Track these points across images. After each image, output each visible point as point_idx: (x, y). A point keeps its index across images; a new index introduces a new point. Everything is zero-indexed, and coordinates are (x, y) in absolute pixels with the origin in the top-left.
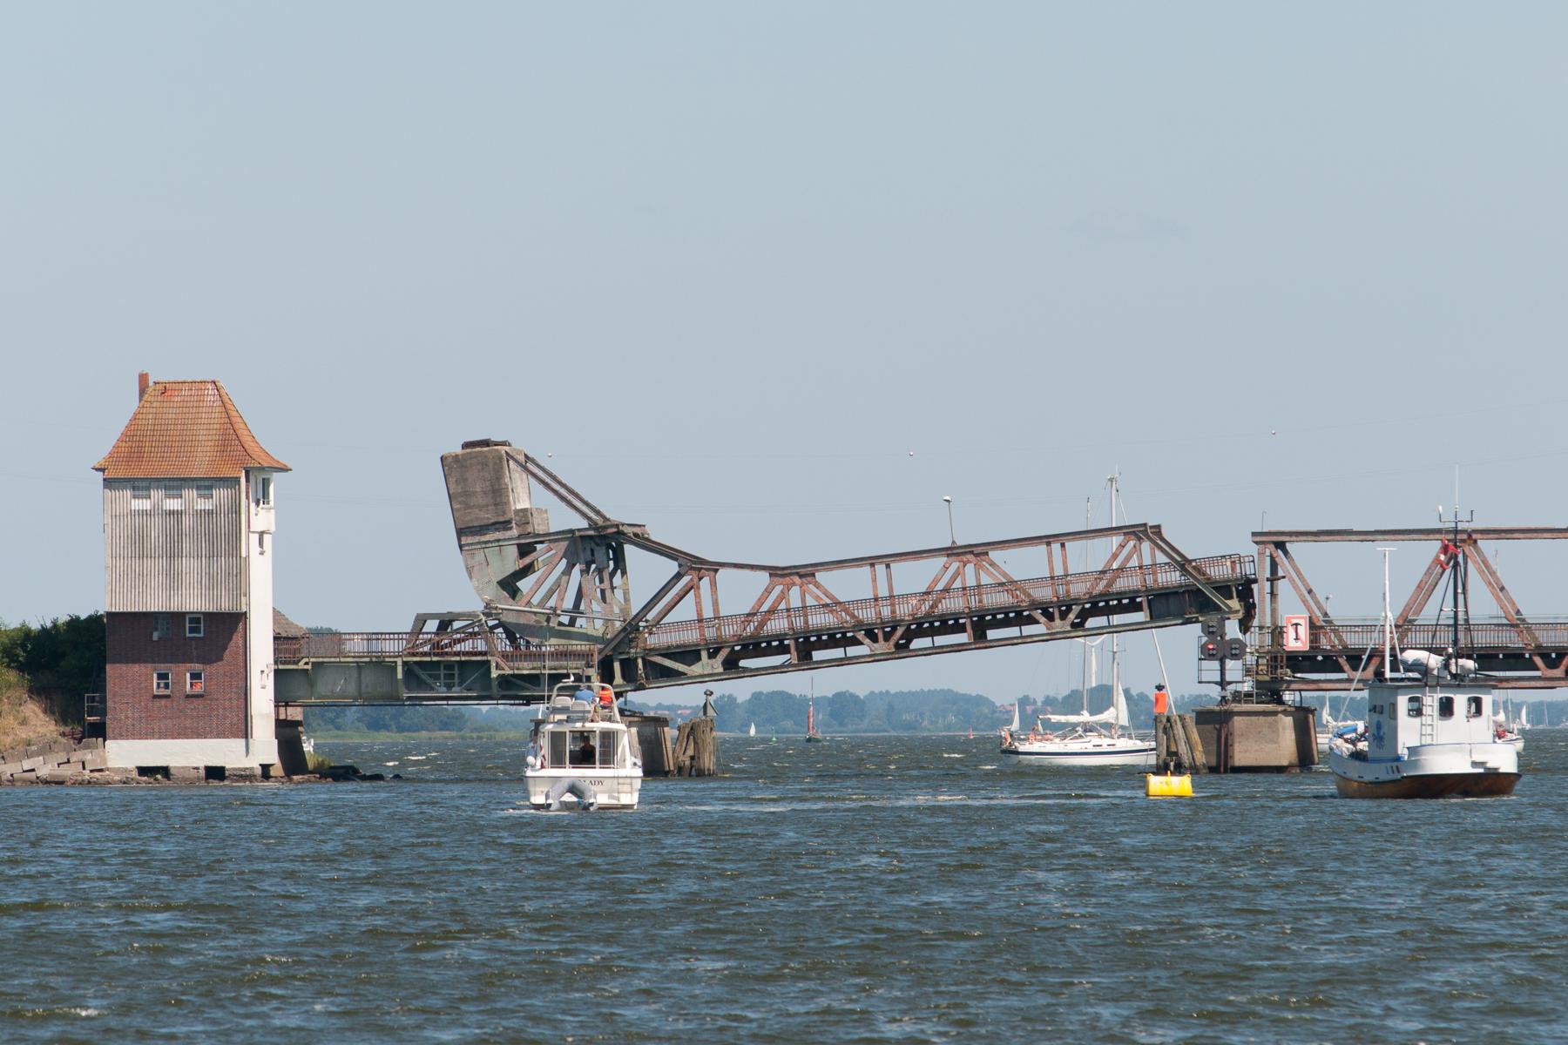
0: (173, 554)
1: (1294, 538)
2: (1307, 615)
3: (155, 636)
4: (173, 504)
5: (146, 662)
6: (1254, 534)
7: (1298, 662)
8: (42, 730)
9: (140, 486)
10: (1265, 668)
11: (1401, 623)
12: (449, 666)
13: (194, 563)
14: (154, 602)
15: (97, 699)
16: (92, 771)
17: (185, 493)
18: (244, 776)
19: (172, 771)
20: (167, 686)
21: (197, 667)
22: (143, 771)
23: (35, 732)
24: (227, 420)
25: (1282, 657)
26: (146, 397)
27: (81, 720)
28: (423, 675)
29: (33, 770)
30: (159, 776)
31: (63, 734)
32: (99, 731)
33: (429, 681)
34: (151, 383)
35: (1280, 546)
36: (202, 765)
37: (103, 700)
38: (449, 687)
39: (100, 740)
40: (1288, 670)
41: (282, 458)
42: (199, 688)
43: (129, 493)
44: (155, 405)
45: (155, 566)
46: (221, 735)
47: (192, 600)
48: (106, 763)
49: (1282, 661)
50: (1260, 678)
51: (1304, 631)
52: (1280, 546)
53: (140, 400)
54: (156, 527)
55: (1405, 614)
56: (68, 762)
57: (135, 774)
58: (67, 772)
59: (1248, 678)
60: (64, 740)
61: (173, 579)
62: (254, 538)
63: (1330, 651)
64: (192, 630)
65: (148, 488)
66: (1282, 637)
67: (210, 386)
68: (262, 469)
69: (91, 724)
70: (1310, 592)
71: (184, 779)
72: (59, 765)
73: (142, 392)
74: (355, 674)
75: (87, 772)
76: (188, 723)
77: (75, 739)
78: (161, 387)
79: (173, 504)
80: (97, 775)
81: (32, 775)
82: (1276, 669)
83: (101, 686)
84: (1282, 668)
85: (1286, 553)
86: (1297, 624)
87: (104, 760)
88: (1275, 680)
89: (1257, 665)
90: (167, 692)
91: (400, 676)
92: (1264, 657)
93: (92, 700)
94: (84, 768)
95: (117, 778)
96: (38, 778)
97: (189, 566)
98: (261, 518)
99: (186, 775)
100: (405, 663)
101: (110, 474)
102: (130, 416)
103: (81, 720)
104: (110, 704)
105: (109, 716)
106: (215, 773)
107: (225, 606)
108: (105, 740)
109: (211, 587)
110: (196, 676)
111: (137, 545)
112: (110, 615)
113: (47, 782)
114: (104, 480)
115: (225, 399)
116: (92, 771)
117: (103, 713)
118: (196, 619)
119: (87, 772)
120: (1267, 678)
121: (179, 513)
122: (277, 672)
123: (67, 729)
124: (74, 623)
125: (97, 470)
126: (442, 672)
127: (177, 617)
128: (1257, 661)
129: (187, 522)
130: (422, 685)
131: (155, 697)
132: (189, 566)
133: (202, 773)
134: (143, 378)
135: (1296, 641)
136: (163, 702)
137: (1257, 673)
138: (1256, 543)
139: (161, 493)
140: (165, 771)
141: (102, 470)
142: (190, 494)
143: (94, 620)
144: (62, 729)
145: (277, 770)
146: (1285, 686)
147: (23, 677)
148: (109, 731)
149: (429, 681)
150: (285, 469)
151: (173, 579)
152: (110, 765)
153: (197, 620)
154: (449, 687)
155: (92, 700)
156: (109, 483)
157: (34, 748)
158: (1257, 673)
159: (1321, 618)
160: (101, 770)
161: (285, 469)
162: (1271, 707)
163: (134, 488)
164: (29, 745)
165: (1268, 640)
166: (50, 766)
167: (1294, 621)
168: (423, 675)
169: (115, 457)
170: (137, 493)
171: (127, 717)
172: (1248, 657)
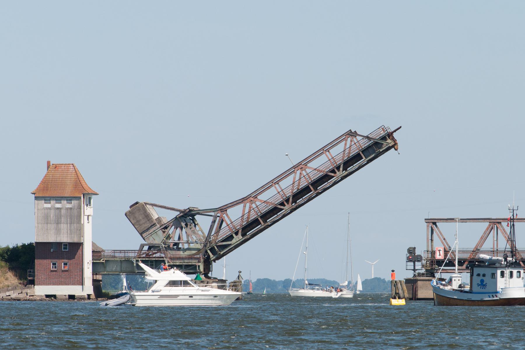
0: (58, 222)
1: (439, 221)
2: (443, 247)
3: (52, 250)
4: (58, 206)
6: (426, 219)
7: (439, 263)
8: (13, 282)
9: (47, 199)
10: (429, 265)
11: (475, 250)
13: (65, 226)
14: (52, 239)
15: (32, 271)
16: (30, 296)
18: (81, 298)
19: (57, 296)
20: (55, 267)
21: (66, 261)
22: (47, 296)
23: (11, 282)
24: (77, 177)
25: (435, 261)
26: (49, 169)
27: (26, 279)
29: (10, 295)
30: (53, 298)
31: (20, 283)
32: (32, 283)
34: (51, 165)
35: (435, 223)
37: (34, 272)
39: (33, 285)
40: (437, 266)
42: (66, 269)
47: (64, 238)
48: (35, 293)
49: (434, 263)
50: (427, 268)
51: (442, 253)
52: (435, 223)
53: (48, 170)
54: (52, 214)
55: (476, 247)
56: (22, 293)
57: (44, 297)
58: (21, 296)
59: (423, 268)
60: (20, 285)
61: (58, 231)
62: (86, 217)
63: (451, 259)
64: (64, 248)
65: (50, 200)
66: (435, 254)
67: (71, 166)
69: (30, 280)
70: (444, 239)
71: (61, 299)
72: (19, 294)
73: (48, 167)
74: (120, 264)
77: (24, 285)
78: (55, 166)
79: (58, 206)
80: (31, 297)
81: (9, 297)
82: (433, 265)
83: (33, 267)
84: (434, 265)
85: (436, 226)
86: (440, 250)
87: (34, 292)
88: (432, 269)
89: (426, 264)
90: (56, 269)
92: (429, 261)
93: (30, 272)
94: (27, 295)
95: (38, 298)
96: (11, 298)
97: (64, 227)
98: (88, 211)
99: (62, 298)
101: (37, 195)
103: (26, 279)
104: (36, 273)
106: (72, 297)
107: (76, 240)
108: (34, 286)
109: (71, 234)
110: (65, 264)
111: (46, 219)
112: (36, 243)
113: (14, 300)
114: (35, 197)
115: (76, 170)
116: (30, 296)
117: (34, 276)
118: (66, 245)
120: (429, 268)
121: (60, 209)
122: (93, 263)
123: (22, 282)
124: (24, 246)
125: (32, 194)
128: (426, 262)
129: (63, 211)
131: (52, 271)
132: (64, 227)
133: (67, 297)
134: (49, 163)
135: (439, 256)
136: (54, 273)
137: (426, 267)
138: (426, 222)
139: (54, 202)
140: (55, 296)
141: (34, 194)
143: (31, 245)
144: (20, 282)
146: (435, 271)
147: (7, 264)
148: (36, 282)
151: (58, 231)
152: (36, 294)
153: (66, 245)
155: (30, 272)
156: (36, 198)
157: (10, 288)
158: (426, 267)
159: (448, 248)
161: (96, 194)
162: (430, 278)
163: (45, 200)
164: (8, 287)
165: (430, 255)
166: (15, 294)
167: (439, 249)
170: (46, 202)
171: (42, 278)
172: (423, 261)
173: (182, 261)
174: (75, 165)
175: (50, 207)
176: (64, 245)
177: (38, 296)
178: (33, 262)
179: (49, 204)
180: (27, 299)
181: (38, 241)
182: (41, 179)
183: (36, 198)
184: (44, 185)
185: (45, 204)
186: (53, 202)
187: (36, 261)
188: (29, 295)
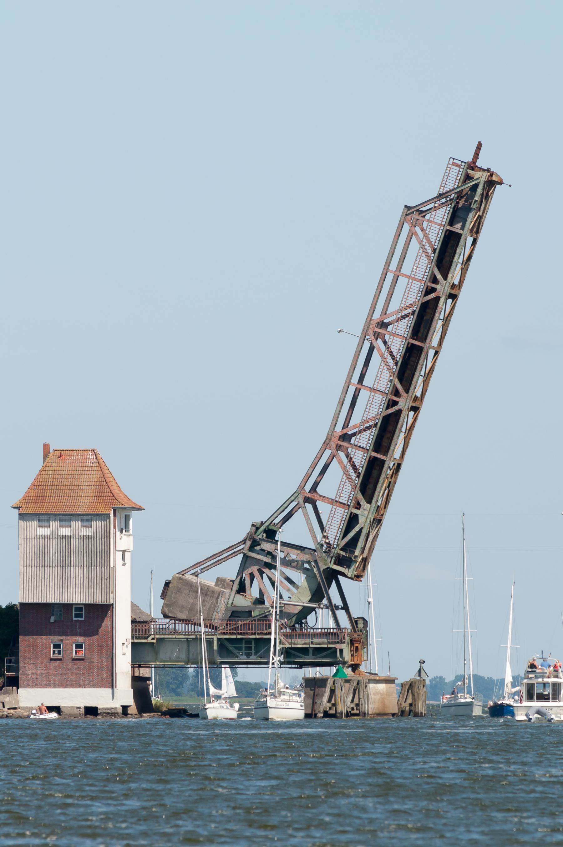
0: (64, 564)
3: (52, 619)
4: (65, 531)
5: (46, 635)
12: (248, 641)
13: (79, 571)
15: (13, 661)
16: (9, 709)
17: (73, 523)
18: (111, 713)
19: (62, 710)
21: (80, 639)
24: (101, 476)
28: (231, 647)
32: (14, 682)
33: (235, 651)
34: (51, 451)
36: (82, 705)
37: (17, 662)
38: (248, 655)
39: (15, 688)
41: (137, 500)
42: (81, 655)
43: (35, 523)
44: (54, 465)
45: (53, 572)
46: (95, 686)
53: (44, 462)
54: (53, 547)
61: (65, 582)
62: (119, 555)
65: (48, 521)
67: (90, 453)
68: (125, 508)
69: (9, 678)
71: (70, 715)
73: (45, 456)
74: (185, 646)
75: (6, 709)
76: (73, 677)
79: (65, 531)
83: (15, 652)
87: (17, 702)
90: (60, 657)
91: (215, 647)
94: (4, 707)
99: (72, 712)
100: (219, 639)
101: (22, 511)
102: (37, 472)
104: (21, 664)
105: (21, 672)
106: (91, 711)
107: (99, 599)
108: (18, 688)
110: (79, 646)
112: (22, 605)
114: (19, 514)
115: (101, 461)
116: (9, 709)
117: (17, 670)
118: (79, 608)
119: (6, 709)
121: (69, 537)
122: (133, 645)
125: (15, 508)
126: (244, 646)
127: (67, 607)
129: (74, 543)
130: (230, 654)
133: (83, 711)
134: (46, 447)
136: (57, 663)
139: (57, 523)
142: (76, 524)
143: (11, 608)
145: (133, 710)
148: (21, 682)
149: (235, 651)
150: (140, 509)
151: (65, 582)
152: (22, 705)
153: (81, 609)
154: (248, 655)
155: (10, 661)
156: (22, 517)
160: (15, 708)
161: (140, 509)
163: (39, 520)
168: (231, 647)
169: (26, 500)
170: (41, 523)
171: (33, 673)
173: (308, 641)
174: (97, 452)
175: (49, 534)
176: (77, 609)
177: (26, 709)
178: (16, 642)
179: (46, 529)
180: (3, 715)
181: (24, 602)
182: (31, 481)
183: (22, 517)
184: (37, 490)
185: (38, 529)
186: (54, 524)
187: (23, 641)
188: (7, 706)
